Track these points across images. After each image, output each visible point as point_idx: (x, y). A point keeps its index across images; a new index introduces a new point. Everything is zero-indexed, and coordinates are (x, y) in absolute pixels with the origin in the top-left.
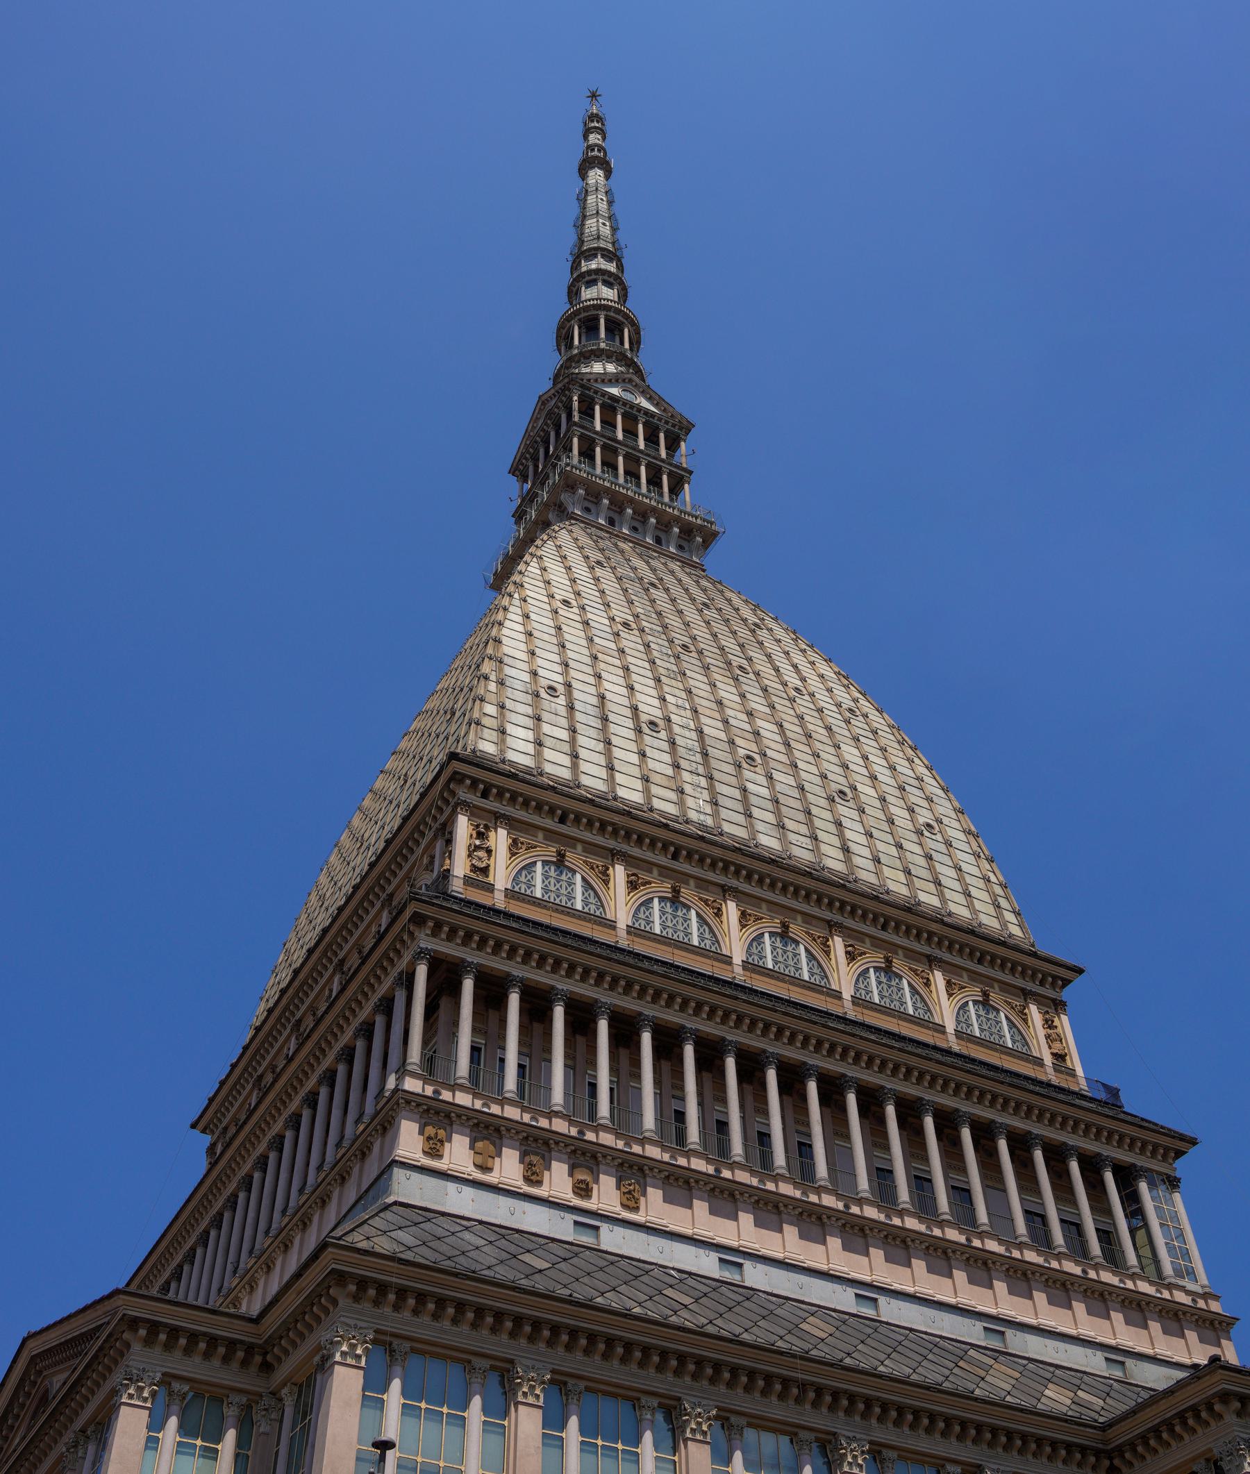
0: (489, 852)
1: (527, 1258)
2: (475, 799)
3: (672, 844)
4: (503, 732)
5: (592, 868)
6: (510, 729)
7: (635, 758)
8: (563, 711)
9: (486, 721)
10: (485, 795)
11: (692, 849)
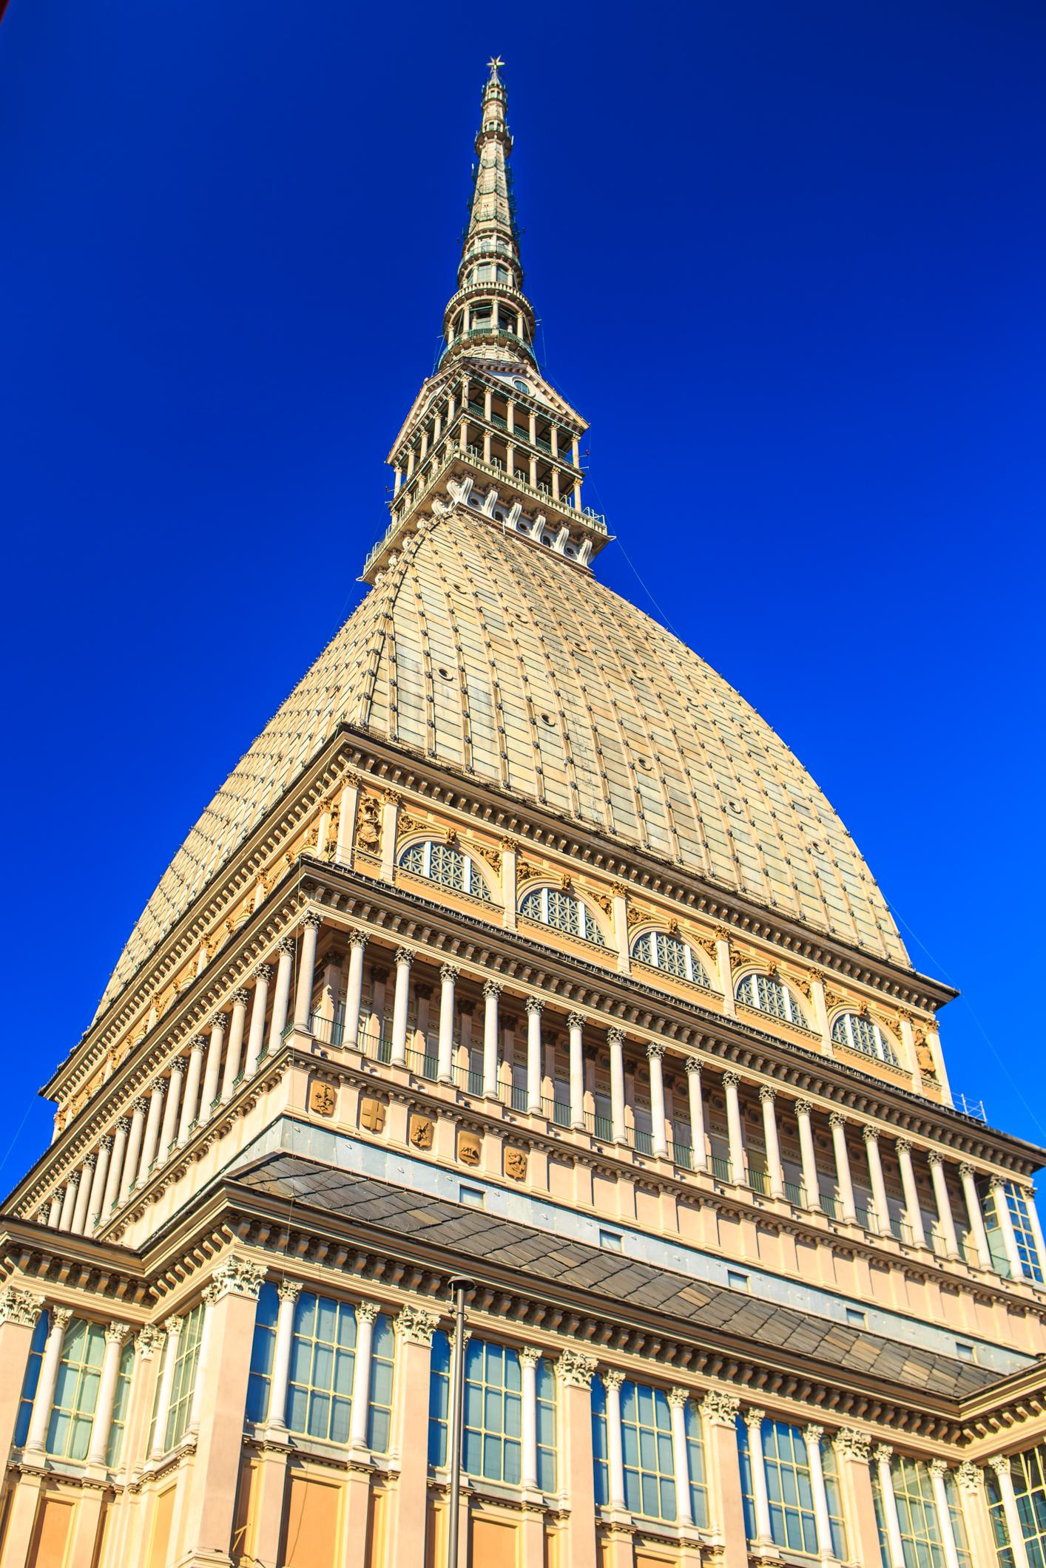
0: (378, 828)
1: (416, 1213)
2: (366, 775)
3: (564, 837)
4: (395, 710)
5: (482, 854)
6: (402, 708)
7: (530, 750)
8: (456, 695)
9: (376, 697)
10: (375, 770)
11: (584, 844)
